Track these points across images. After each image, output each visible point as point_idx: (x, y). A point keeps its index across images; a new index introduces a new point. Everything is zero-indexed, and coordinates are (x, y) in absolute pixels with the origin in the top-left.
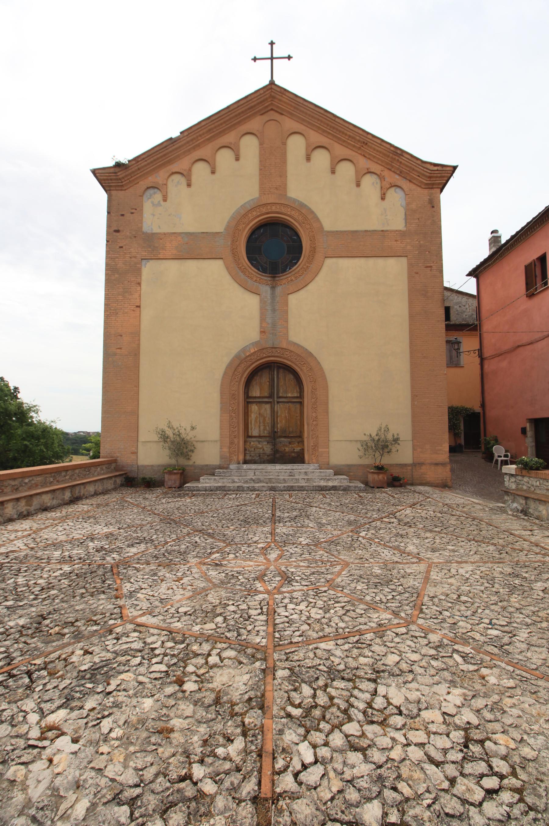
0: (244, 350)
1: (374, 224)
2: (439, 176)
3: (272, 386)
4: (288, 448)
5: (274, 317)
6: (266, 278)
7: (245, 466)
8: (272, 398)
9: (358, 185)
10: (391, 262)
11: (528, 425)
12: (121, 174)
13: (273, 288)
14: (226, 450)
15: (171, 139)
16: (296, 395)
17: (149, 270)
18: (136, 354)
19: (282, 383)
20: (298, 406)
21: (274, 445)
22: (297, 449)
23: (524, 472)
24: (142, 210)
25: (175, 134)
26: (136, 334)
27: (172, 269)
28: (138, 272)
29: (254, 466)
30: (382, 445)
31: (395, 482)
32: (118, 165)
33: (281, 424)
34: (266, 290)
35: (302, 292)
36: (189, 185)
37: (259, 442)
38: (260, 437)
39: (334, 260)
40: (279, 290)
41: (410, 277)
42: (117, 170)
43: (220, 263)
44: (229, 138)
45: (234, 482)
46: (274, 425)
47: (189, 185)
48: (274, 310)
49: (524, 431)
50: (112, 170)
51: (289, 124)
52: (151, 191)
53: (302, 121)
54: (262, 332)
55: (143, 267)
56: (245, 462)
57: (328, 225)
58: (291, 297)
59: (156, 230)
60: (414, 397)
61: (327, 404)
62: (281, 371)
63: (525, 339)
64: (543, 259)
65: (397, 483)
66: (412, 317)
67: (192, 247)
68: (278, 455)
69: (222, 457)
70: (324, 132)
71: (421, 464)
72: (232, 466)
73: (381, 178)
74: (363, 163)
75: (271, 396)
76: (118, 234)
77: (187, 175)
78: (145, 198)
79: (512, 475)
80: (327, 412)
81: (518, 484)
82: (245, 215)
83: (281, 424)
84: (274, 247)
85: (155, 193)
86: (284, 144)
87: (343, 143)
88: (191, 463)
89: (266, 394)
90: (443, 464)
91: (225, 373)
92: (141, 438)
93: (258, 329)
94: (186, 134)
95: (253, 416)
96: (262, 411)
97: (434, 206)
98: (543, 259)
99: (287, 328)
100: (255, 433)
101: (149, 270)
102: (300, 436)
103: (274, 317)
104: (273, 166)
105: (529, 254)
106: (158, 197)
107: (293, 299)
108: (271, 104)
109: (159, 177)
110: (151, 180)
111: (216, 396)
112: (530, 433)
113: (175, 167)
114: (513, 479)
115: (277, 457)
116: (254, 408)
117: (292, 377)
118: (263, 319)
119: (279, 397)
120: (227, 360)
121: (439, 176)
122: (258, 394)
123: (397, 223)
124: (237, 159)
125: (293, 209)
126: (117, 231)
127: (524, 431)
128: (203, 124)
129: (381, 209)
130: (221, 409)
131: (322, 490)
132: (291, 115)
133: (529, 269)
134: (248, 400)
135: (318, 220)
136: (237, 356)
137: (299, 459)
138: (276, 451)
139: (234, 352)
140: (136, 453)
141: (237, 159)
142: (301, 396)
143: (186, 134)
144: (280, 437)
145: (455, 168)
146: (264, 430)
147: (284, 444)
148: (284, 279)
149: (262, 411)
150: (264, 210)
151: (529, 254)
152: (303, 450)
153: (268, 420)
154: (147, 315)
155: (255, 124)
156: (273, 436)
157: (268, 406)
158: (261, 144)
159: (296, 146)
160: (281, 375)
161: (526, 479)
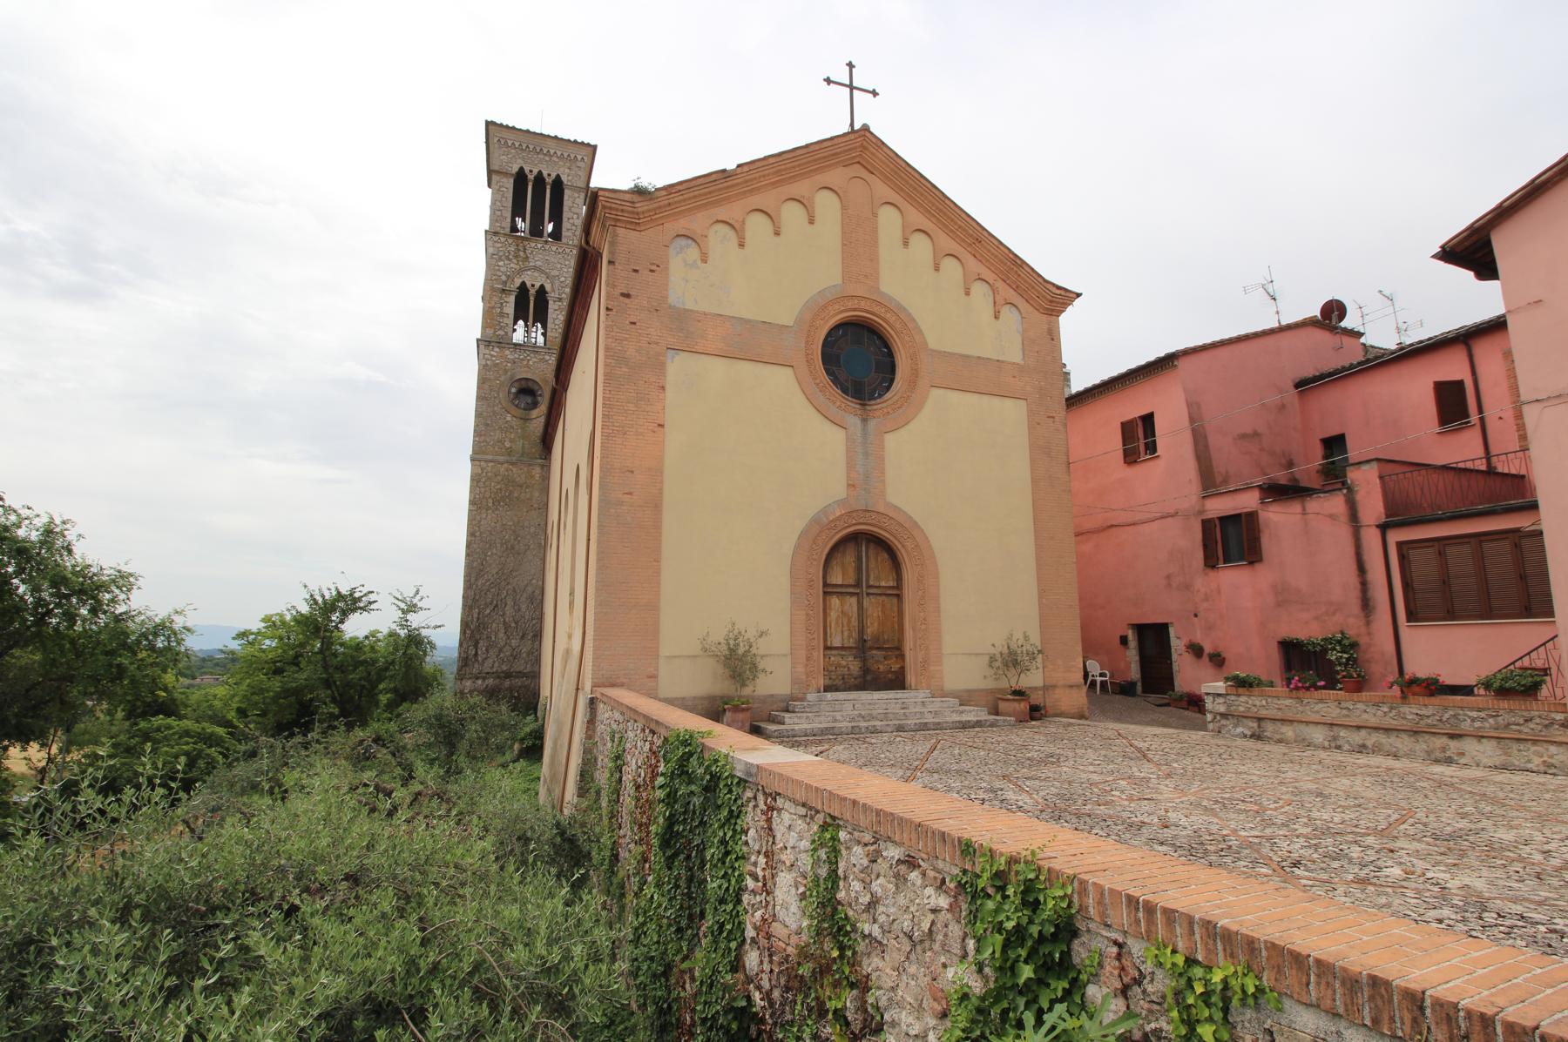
0: (825, 510)
1: (985, 349)
2: (1061, 298)
3: (859, 569)
4: (883, 667)
5: (865, 465)
6: (853, 405)
7: (829, 695)
8: (858, 588)
9: (968, 294)
10: (1009, 403)
11: (1130, 634)
12: (642, 206)
13: (865, 421)
14: (800, 669)
15: (724, 171)
16: (891, 584)
17: (678, 367)
18: (656, 505)
19: (872, 564)
20: (895, 600)
21: (864, 660)
22: (896, 667)
23: (1241, 690)
24: (667, 269)
25: (731, 166)
26: (657, 473)
27: (716, 370)
28: (661, 368)
29: (841, 695)
30: (1012, 660)
31: (1036, 713)
32: (639, 191)
33: (871, 629)
34: (854, 421)
35: (902, 431)
36: (741, 245)
37: (842, 656)
38: (843, 648)
39: (941, 391)
40: (872, 424)
41: (1031, 428)
42: (636, 198)
43: (789, 371)
44: (800, 188)
45: (836, 721)
46: (862, 631)
47: (741, 245)
48: (866, 454)
49: (1124, 640)
50: (627, 197)
51: (883, 190)
52: (683, 242)
53: (898, 190)
54: (851, 486)
55: (669, 362)
56: (827, 689)
57: (933, 343)
58: (888, 437)
59: (690, 305)
60: (1042, 593)
61: (937, 598)
62: (872, 546)
63: (1123, 517)
64: (1148, 420)
65: (1037, 714)
66: (1034, 481)
67: (747, 343)
68: (869, 678)
69: (794, 682)
70: (927, 212)
71: (1054, 687)
72: (811, 697)
73: (994, 291)
74: (972, 263)
75: (858, 584)
76: (627, 300)
77: (738, 229)
78: (672, 251)
79: (1219, 695)
80: (938, 609)
81: (1229, 706)
82: (824, 307)
83: (871, 629)
84: (859, 358)
85: (688, 246)
86: (875, 215)
87: (951, 234)
88: (747, 691)
89: (852, 582)
90: (1078, 686)
91: (798, 546)
92: (665, 651)
93: (844, 482)
94: (746, 169)
95: (833, 615)
96: (846, 607)
97: (1053, 336)
98: (1148, 420)
99: (883, 482)
100: (837, 642)
101: (678, 367)
102: (898, 651)
103: (865, 465)
104: (858, 244)
105: (1130, 406)
106: (693, 253)
107: (891, 440)
108: (859, 153)
109: (695, 222)
110: (681, 224)
111: (785, 582)
112: (1133, 642)
113: (722, 212)
114: (1221, 700)
115: (869, 681)
116: (835, 601)
117: (886, 556)
118: (850, 466)
119: (869, 587)
120: (800, 525)
121: (1058, 299)
122: (840, 582)
123: (1014, 355)
124: (811, 222)
125: (889, 310)
126: (627, 296)
127: (1124, 640)
128: (771, 160)
129: (995, 334)
130: (792, 603)
131: (964, 728)
132: (886, 179)
133: (1127, 429)
134: (828, 590)
135: (920, 332)
136: (815, 520)
137: (897, 682)
138: (865, 670)
139: (811, 513)
140: (654, 677)
141: (811, 222)
142: (899, 585)
143: (746, 169)
144: (871, 648)
145: (1079, 295)
146: (850, 636)
147: (876, 663)
148: (878, 406)
149: (846, 607)
150: (850, 304)
151: (1130, 406)
152: (903, 668)
153: (854, 622)
154: (674, 441)
155: (836, 176)
156: (862, 648)
157: (854, 600)
158: (844, 208)
159: (889, 222)
160: (871, 552)
161: (1243, 699)
